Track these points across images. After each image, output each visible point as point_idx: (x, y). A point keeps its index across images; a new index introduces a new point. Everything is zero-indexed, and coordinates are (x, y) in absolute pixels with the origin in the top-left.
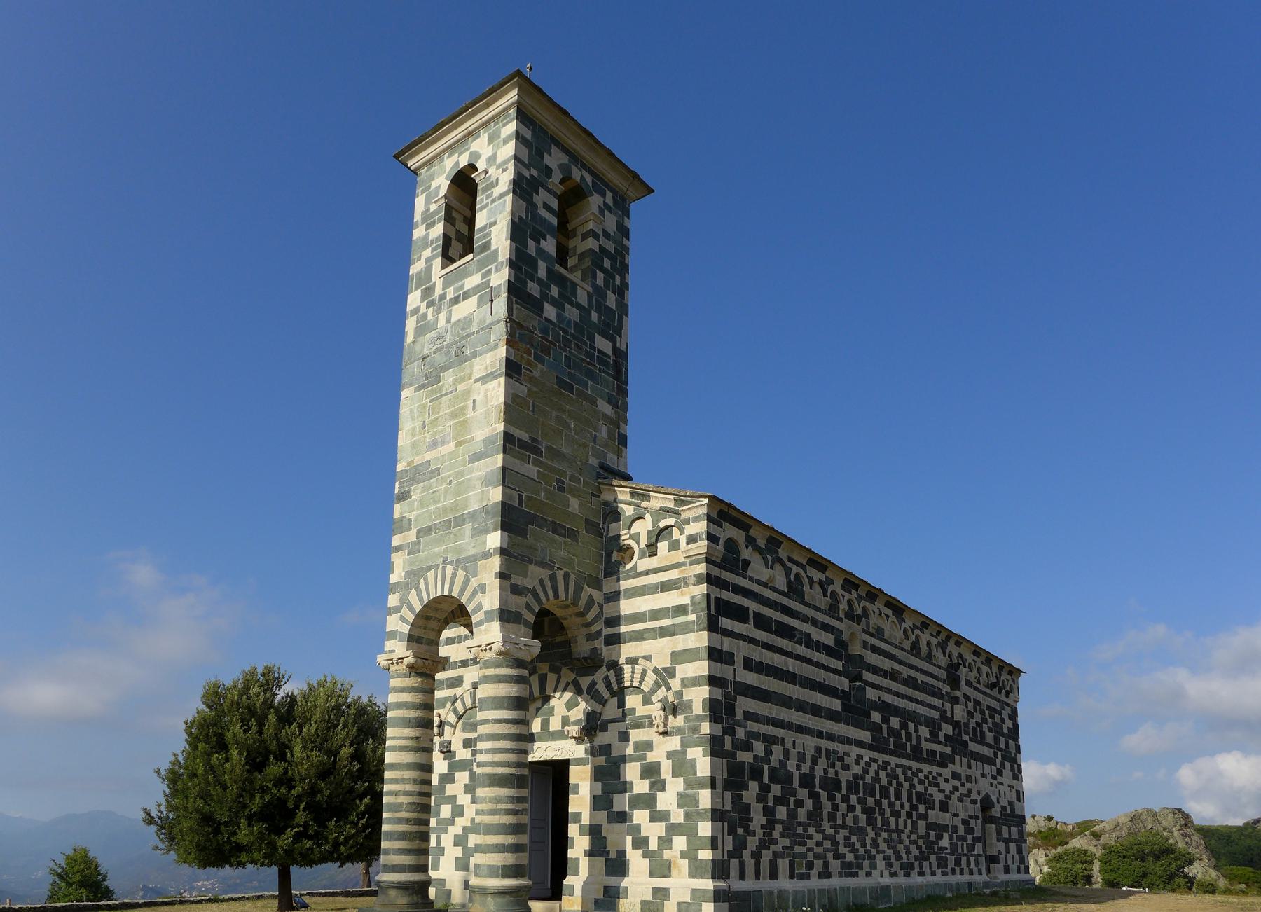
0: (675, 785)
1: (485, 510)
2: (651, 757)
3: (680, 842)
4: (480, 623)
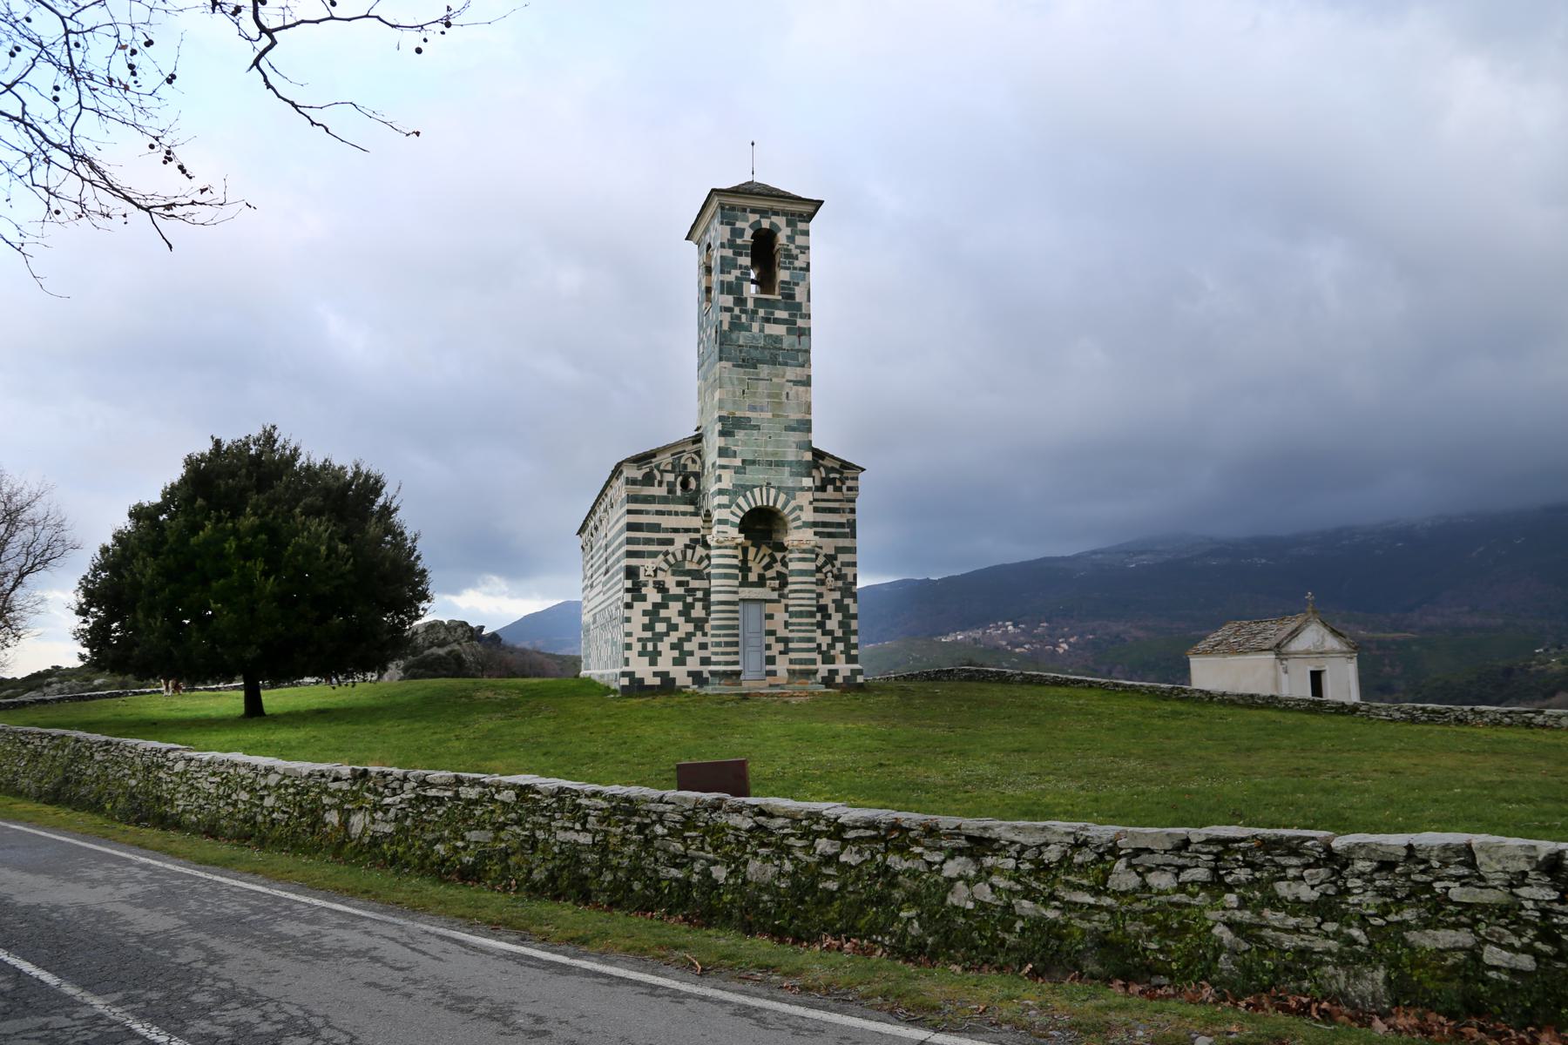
0: (837, 617)
1: (799, 463)
2: (822, 602)
3: (840, 646)
4: (798, 528)
